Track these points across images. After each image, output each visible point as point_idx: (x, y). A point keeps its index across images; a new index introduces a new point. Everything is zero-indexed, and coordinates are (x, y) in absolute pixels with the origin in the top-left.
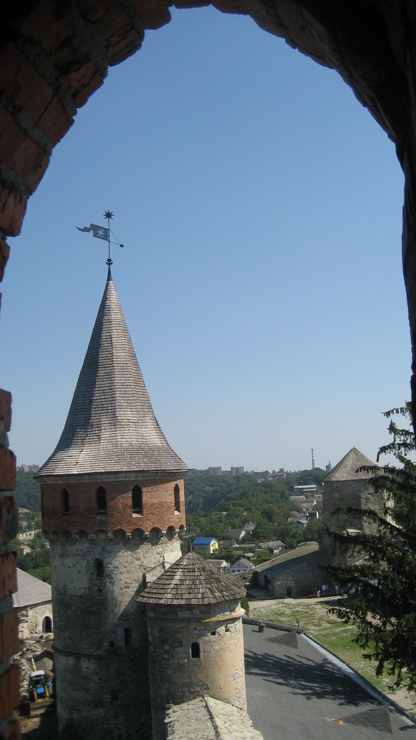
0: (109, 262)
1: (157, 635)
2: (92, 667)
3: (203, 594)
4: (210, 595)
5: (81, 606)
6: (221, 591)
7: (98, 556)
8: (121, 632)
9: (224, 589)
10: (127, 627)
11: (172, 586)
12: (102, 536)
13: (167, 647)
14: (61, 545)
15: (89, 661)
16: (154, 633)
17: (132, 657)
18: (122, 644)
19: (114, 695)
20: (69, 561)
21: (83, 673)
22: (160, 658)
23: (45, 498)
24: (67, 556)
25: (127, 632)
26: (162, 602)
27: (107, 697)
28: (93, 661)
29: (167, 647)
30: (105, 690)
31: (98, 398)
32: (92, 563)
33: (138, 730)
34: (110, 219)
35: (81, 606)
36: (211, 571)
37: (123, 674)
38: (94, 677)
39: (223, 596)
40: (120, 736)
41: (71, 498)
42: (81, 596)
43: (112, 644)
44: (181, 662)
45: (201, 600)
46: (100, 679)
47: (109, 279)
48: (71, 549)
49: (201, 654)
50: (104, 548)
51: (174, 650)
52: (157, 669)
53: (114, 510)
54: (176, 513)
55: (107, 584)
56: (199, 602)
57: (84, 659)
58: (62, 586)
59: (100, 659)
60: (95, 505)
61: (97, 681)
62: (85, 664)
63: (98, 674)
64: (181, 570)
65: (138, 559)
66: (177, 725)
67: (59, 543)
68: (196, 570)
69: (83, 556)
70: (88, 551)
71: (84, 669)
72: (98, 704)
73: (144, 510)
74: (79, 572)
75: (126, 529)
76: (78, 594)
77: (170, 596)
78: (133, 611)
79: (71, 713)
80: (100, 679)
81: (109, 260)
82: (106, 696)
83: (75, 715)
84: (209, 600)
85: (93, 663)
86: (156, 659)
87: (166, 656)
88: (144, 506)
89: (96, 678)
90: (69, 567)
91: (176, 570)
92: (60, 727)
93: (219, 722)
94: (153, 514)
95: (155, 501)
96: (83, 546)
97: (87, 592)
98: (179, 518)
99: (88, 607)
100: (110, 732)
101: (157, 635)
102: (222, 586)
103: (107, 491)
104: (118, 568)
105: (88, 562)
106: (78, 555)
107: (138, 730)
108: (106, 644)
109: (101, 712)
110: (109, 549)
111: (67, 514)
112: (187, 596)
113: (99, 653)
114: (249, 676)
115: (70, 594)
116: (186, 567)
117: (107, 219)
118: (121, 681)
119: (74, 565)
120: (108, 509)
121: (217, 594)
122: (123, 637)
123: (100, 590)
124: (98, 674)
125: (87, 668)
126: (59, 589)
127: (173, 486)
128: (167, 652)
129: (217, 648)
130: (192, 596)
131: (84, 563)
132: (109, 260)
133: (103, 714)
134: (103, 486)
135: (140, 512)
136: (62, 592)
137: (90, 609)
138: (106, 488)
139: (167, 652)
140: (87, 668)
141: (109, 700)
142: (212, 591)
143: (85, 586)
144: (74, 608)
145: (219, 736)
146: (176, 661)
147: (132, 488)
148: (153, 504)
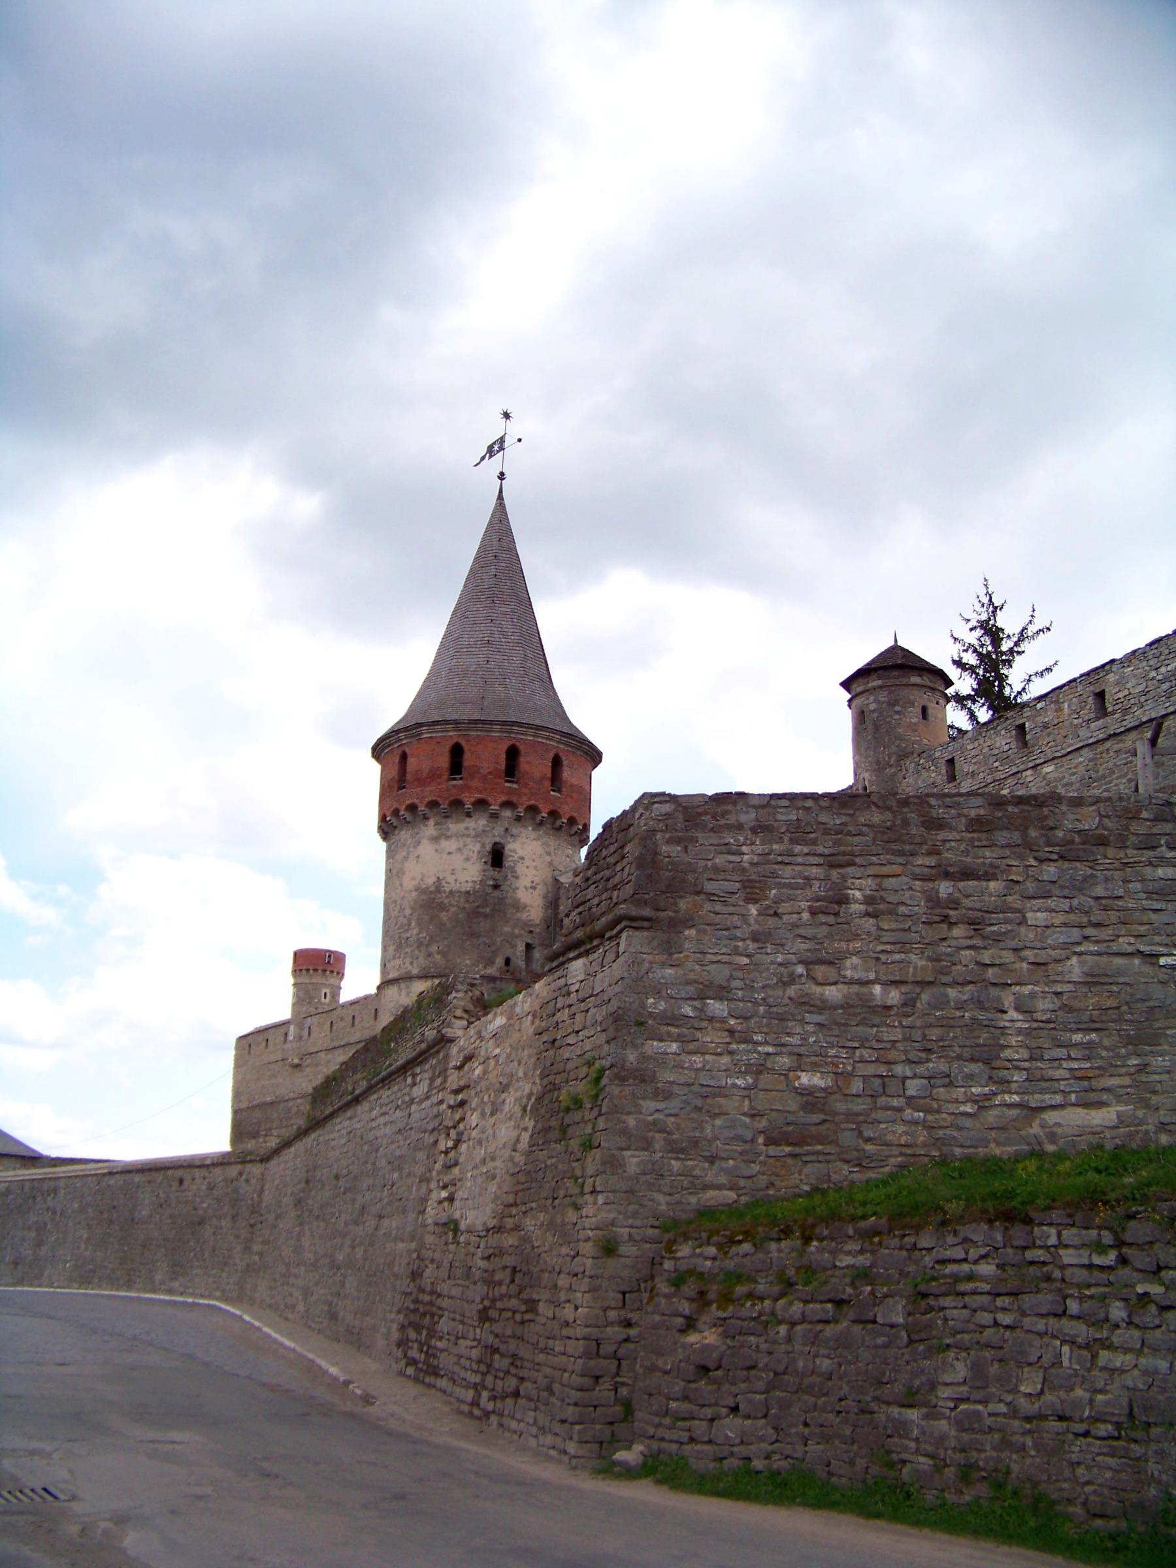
5: (467, 905)
7: (498, 839)
8: (521, 947)
10: (529, 941)
12: (507, 813)
13: (897, 708)
18: (521, 963)
20: (447, 845)
24: (448, 838)
25: (529, 947)
29: (897, 708)
32: (488, 848)
35: (467, 905)
41: (467, 756)
42: (468, 892)
43: (508, 961)
48: (453, 827)
50: (507, 830)
60: (502, 765)
67: (431, 822)
69: (476, 836)
70: (484, 831)
74: (468, 859)
76: (463, 890)
78: (537, 922)
81: (502, 474)
87: (897, 717)
90: (449, 853)
96: (480, 822)
105: (483, 845)
106: (468, 836)
108: (500, 961)
110: (514, 831)
115: (447, 890)
119: (459, 850)
128: (898, 713)
131: (478, 847)
132: (502, 474)
135: (559, 791)
137: (481, 910)
138: (521, 747)
139: (898, 713)
144: (453, 909)
147: (552, 755)
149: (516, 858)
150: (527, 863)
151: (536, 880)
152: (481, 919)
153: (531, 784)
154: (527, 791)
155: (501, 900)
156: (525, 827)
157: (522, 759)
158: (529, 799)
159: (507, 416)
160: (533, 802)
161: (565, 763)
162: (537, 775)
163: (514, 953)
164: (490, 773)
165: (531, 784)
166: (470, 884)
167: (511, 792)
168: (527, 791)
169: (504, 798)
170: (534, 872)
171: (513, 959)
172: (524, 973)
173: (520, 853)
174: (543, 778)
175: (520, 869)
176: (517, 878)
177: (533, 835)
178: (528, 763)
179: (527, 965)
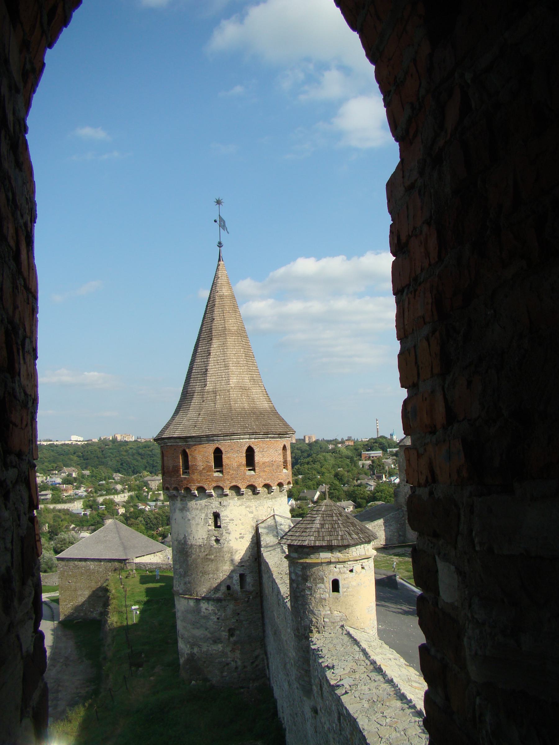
0: (220, 245)
1: (300, 573)
2: (211, 608)
3: (342, 536)
4: (348, 537)
6: (357, 534)
9: (360, 532)
10: (242, 572)
11: (313, 530)
14: (181, 500)
15: (208, 603)
16: (297, 571)
17: (246, 599)
18: (237, 587)
19: (231, 632)
21: (203, 613)
22: (302, 593)
23: (165, 458)
25: (242, 577)
26: (306, 543)
27: (225, 634)
28: (211, 602)
30: (222, 628)
31: (213, 367)
33: (253, 663)
34: (221, 205)
36: (347, 516)
37: (239, 614)
38: (212, 617)
39: (360, 538)
40: (237, 668)
41: (190, 457)
42: (200, 546)
43: (229, 588)
44: (322, 596)
45: (340, 541)
46: (218, 619)
47: (219, 260)
49: (341, 589)
51: (316, 585)
52: (300, 603)
53: (230, 468)
54: (285, 471)
55: (224, 533)
56: (339, 542)
57: (204, 601)
58: (182, 537)
59: (219, 600)
61: (216, 620)
62: (204, 605)
63: (216, 614)
64: (320, 515)
65: (252, 512)
66: (325, 651)
67: (179, 499)
68: (334, 515)
71: (203, 610)
72: (216, 641)
73: (256, 468)
75: (240, 485)
76: (198, 544)
77: (312, 538)
79: (193, 648)
80: (218, 619)
81: (220, 243)
82: (224, 633)
83: (196, 650)
84: (348, 541)
85: (212, 605)
86: (298, 594)
88: (256, 465)
89: (214, 618)
91: (316, 516)
92: (182, 661)
93: (364, 645)
94: (264, 471)
95: (266, 460)
97: (205, 542)
98: (287, 475)
99: (206, 555)
100: (228, 664)
101: (300, 573)
102: (358, 529)
103: (223, 452)
104: (233, 520)
105: (207, 515)
106: (197, 509)
107: (253, 663)
109: (220, 647)
110: (225, 503)
111: (186, 472)
112: (328, 538)
113: (217, 595)
114: (380, 608)
116: (324, 513)
117: (218, 205)
118: (237, 620)
120: (224, 467)
121: (355, 536)
122: (238, 581)
123: (217, 541)
124: (216, 614)
125: (206, 609)
126: (179, 539)
127: (282, 446)
129: (354, 583)
130: (332, 538)
132: (220, 243)
133: (221, 648)
134: (220, 447)
136: (183, 542)
137: (208, 557)
138: (222, 449)
140: (206, 609)
141: (227, 637)
142: (350, 534)
143: (204, 537)
145: (370, 657)
146: (319, 596)
147: (246, 448)
148: (264, 463)
149: (228, 521)
150: (235, 522)
151: (243, 532)
152: (209, 563)
153: (232, 472)
154: (229, 477)
155: (220, 550)
156: (233, 498)
157: (224, 456)
158: (231, 482)
159: (218, 202)
160: (234, 484)
161: (256, 451)
162: (235, 465)
163: (232, 582)
164: (203, 469)
165: (232, 472)
166: (201, 541)
167: (218, 479)
168: (229, 477)
169: (214, 484)
170: (242, 527)
171: (231, 586)
172: (239, 593)
173: (231, 516)
174: (239, 466)
175: (231, 527)
176: (229, 534)
177: (239, 502)
178: (228, 458)
179: (242, 586)
